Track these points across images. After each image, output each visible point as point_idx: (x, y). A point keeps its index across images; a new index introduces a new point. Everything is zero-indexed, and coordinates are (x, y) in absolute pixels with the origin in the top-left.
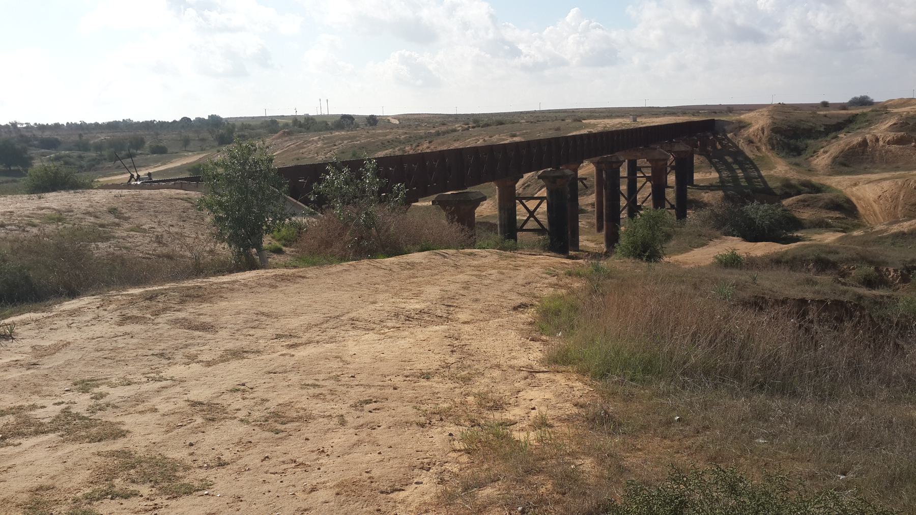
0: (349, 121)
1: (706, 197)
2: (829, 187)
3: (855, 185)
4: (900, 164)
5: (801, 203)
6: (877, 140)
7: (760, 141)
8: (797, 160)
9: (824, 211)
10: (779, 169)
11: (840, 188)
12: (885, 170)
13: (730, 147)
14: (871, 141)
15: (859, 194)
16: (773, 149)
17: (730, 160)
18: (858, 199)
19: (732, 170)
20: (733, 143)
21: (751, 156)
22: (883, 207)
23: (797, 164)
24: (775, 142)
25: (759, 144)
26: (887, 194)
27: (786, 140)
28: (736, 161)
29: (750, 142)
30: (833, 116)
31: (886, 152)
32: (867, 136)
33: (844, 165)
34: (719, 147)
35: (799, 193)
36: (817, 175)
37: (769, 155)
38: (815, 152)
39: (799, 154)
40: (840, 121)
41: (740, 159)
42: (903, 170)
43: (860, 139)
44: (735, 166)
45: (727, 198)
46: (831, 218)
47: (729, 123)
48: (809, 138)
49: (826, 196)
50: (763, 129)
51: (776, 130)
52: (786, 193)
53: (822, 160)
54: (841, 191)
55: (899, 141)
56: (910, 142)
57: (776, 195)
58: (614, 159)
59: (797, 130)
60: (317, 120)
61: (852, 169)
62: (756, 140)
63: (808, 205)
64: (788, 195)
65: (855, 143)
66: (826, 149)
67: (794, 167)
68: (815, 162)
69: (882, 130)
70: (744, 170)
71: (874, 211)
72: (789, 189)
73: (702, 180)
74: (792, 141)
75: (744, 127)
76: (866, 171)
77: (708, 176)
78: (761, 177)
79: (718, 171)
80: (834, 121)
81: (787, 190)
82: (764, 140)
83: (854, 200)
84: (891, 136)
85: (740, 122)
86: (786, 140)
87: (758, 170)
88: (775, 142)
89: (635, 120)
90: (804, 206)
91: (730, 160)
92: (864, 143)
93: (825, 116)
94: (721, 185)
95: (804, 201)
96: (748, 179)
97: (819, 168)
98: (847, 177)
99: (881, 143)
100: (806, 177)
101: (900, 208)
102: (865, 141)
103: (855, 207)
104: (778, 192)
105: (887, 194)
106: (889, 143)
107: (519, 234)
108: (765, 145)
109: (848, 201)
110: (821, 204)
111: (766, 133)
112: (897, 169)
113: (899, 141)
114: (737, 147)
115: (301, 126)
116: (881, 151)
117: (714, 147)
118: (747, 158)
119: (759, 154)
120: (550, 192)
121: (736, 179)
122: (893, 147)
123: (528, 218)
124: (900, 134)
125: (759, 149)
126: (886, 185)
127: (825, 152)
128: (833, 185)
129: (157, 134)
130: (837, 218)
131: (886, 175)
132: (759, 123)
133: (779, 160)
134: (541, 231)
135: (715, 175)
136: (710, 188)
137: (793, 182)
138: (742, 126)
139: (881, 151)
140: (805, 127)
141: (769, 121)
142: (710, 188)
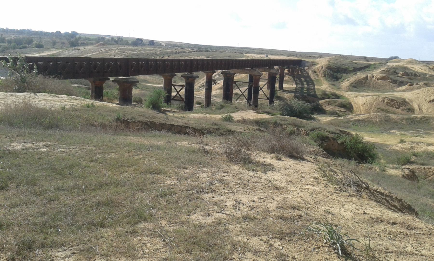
0: (140, 42)
1: (286, 96)
2: (344, 97)
3: (356, 97)
5: (327, 103)
6: (373, 77)
7: (319, 72)
9: (337, 107)
10: (324, 86)
11: (349, 97)
12: (373, 91)
13: (305, 74)
14: (370, 77)
15: (356, 101)
17: (303, 79)
18: (355, 103)
19: (302, 84)
20: (306, 72)
21: (313, 79)
22: (365, 108)
23: (334, 85)
24: (326, 73)
26: (368, 102)
28: (306, 81)
29: (315, 72)
30: (360, 64)
33: (355, 87)
34: (300, 73)
35: (329, 98)
37: (322, 79)
38: (343, 80)
39: (337, 80)
41: (308, 79)
43: (365, 76)
44: (305, 83)
45: (296, 97)
46: (340, 111)
47: (308, 62)
48: (344, 73)
50: (322, 67)
51: (329, 68)
52: (323, 97)
53: (345, 84)
54: (348, 99)
57: (318, 98)
58: (228, 73)
59: (338, 69)
60: (124, 39)
62: (318, 71)
63: (330, 104)
64: (324, 98)
66: (348, 79)
67: (331, 86)
68: (342, 85)
69: (377, 73)
70: (308, 85)
71: (360, 110)
72: (325, 96)
73: (288, 88)
74: (335, 74)
75: (314, 65)
76: (364, 91)
77: (291, 86)
78: (314, 89)
79: (296, 84)
80: (359, 66)
81: (324, 96)
82: (322, 72)
83: (353, 104)
84: (379, 76)
85: (313, 62)
86: (332, 73)
87: (314, 85)
89: (267, 56)
91: (303, 79)
92: (367, 77)
93: (356, 63)
94: (295, 91)
95: (329, 102)
96: (308, 89)
97: (343, 87)
99: (374, 79)
102: (367, 77)
104: (319, 97)
105: (368, 102)
107: (172, 101)
108: (322, 74)
109: (350, 104)
110: (336, 104)
113: (383, 78)
114: (308, 74)
115: (115, 41)
116: (373, 82)
117: (298, 73)
118: (311, 80)
119: (317, 78)
120: (187, 84)
121: (302, 88)
122: (380, 81)
123: (177, 94)
125: (318, 76)
126: (369, 98)
127: (348, 80)
128: (346, 96)
129: (40, 38)
130: (342, 111)
131: (372, 94)
132: (322, 63)
134: (181, 100)
135: (295, 86)
136: (289, 92)
140: (343, 67)
141: (327, 63)
142: (289, 92)
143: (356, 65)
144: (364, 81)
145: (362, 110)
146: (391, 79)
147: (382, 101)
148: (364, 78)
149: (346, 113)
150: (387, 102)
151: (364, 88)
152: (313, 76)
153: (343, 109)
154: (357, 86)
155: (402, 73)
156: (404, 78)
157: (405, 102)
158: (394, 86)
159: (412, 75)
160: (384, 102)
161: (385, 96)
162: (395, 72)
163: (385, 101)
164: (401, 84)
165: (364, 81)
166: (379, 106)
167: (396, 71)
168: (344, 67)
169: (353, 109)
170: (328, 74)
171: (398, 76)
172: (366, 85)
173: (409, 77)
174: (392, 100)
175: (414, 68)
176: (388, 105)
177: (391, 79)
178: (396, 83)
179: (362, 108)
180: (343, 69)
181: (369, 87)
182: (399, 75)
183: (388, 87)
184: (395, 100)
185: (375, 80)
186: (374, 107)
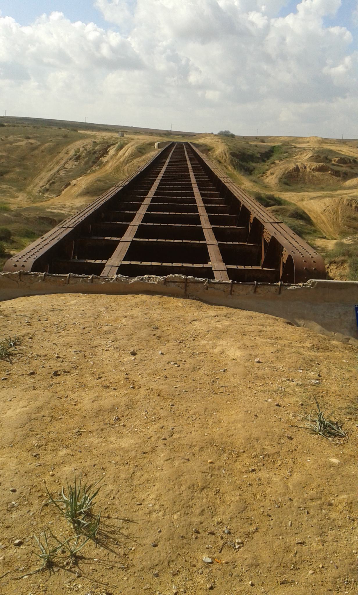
2: (285, 201)
3: (302, 200)
4: (322, 186)
6: (305, 168)
7: (225, 162)
8: (251, 177)
11: (293, 202)
12: (315, 190)
16: (235, 168)
18: (309, 211)
22: (328, 217)
24: (235, 163)
25: (225, 164)
27: (241, 162)
31: (313, 176)
32: (298, 164)
36: (272, 191)
38: (264, 173)
39: (251, 174)
40: (267, 150)
42: (327, 190)
43: (294, 166)
48: (253, 161)
49: (291, 208)
50: (225, 153)
53: (272, 179)
55: (320, 169)
59: (250, 156)
61: (291, 188)
65: (291, 168)
66: (271, 170)
67: (255, 184)
68: (267, 180)
71: (323, 221)
75: (209, 150)
80: (263, 151)
82: (228, 161)
83: (306, 211)
84: (315, 165)
88: (235, 163)
92: (297, 169)
93: (256, 146)
98: (293, 194)
99: (308, 170)
100: (268, 193)
101: (340, 219)
103: (309, 217)
105: (329, 208)
106: (313, 170)
111: (227, 156)
112: (322, 189)
113: (320, 169)
122: (317, 173)
124: (322, 164)
126: (327, 201)
127: (272, 174)
128: (287, 199)
131: (320, 194)
133: (243, 178)
137: (263, 196)
138: (207, 149)
139: (309, 176)
140: (249, 153)
141: (226, 147)
145: (325, 221)
146: (332, 170)
147: (348, 205)
149: (306, 227)
151: (300, 186)
153: (301, 222)
154: (288, 182)
155: (337, 159)
156: (342, 166)
159: (350, 162)
160: (351, 206)
161: (350, 198)
162: (326, 158)
163: (354, 205)
164: (346, 176)
165: (295, 173)
166: (348, 214)
167: (329, 157)
168: (250, 152)
169: (311, 220)
170: (237, 165)
171: (333, 165)
172: (300, 180)
173: (349, 165)
175: (341, 151)
177: (332, 170)
178: (339, 176)
179: (323, 218)
180: (248, 155)
181: (304, 183)
182: (333, 162)
183: (331, 181)
186: (340, 215)
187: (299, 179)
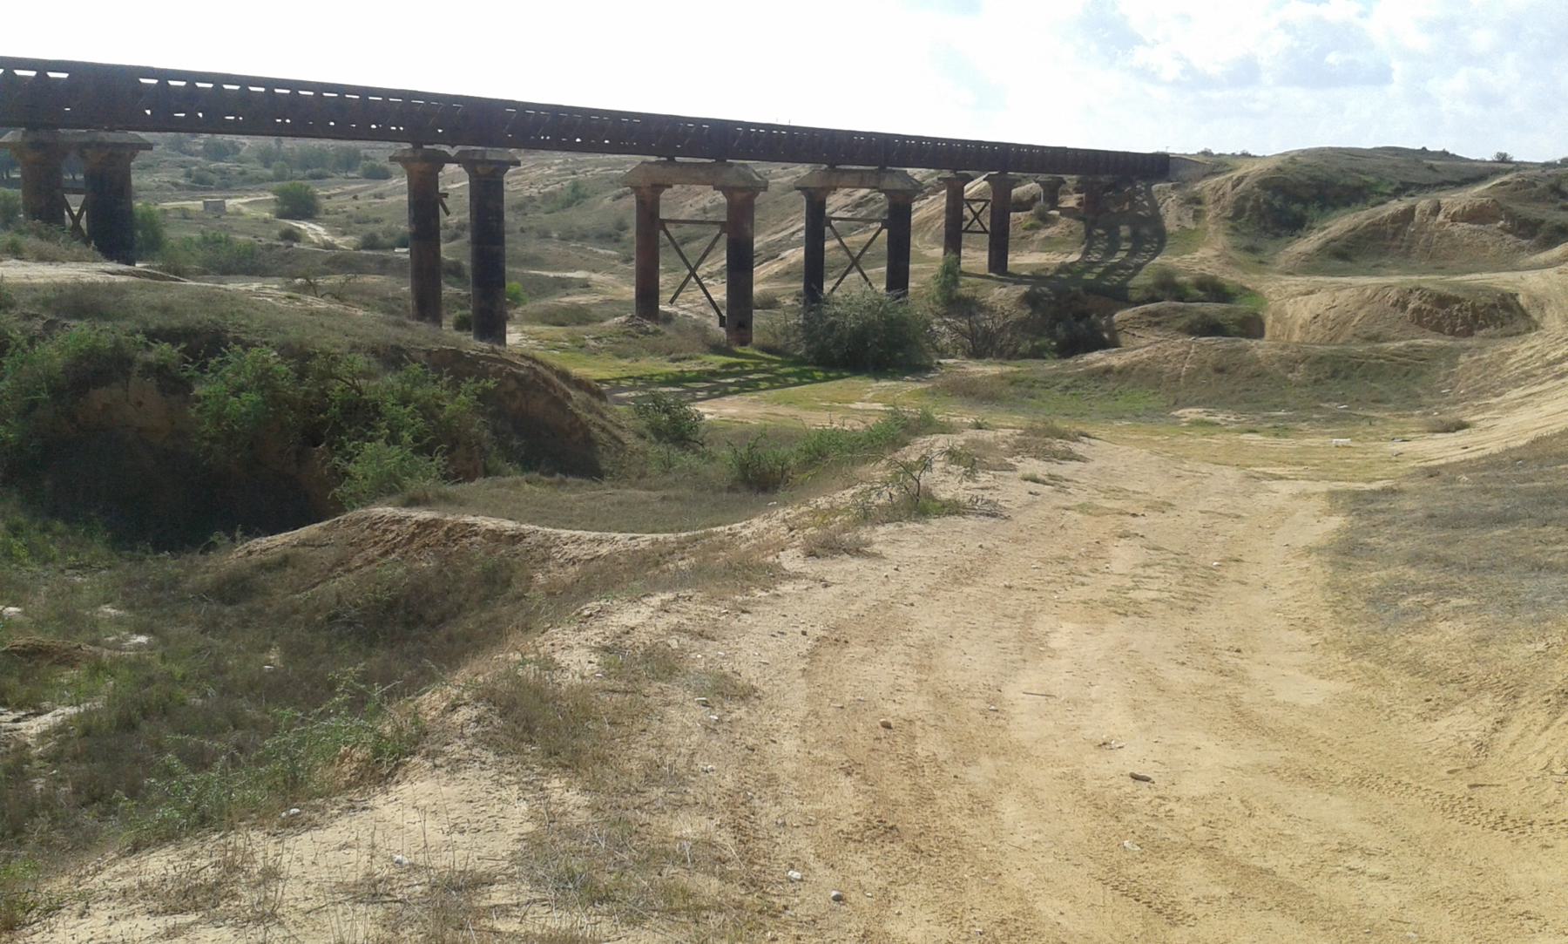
5: (1146, 319)
6: (1437, 209)
14: (1423, 212)
18: (1280, 318)
23: (1252, 250)
24: (1249, 205)
26: (1332, 314)
37: (1212, 228)
41: (1145, 231)
56: (1496, 218)
63: (1158, 324)
70: (1132, 253)
74: (1296, 208)
82: (1230, 198)
83: (1269, 320)
90: (1150, 324)
92: (1409, 213)
93: (1431, 167)
95: (1155, 314)
99: (1440, 218)
104: (1135, 295)
106: (1454, 219)
110: (1181, 323)
116: (1432, 233)
122: (1462, 228)
139: (1432, 233)
140: (1349, 181)
142: (1018, 279)
143: (1429, 173)
144: (1390, 229)
146: (1511, 216)
147: (1394, 305)
148: (1394, 218)
150: (1417, 311)
152: (1172, 214)
157: (1507, 307)
158: (1521, 248)
160: (1404, 307)
165: (1390, 229)
174: (1442, 301)
176: (1419, 323)
184: (1457, 300)
185: (1443, 224)
186: (1350, 330)
187: (1396, 243)
